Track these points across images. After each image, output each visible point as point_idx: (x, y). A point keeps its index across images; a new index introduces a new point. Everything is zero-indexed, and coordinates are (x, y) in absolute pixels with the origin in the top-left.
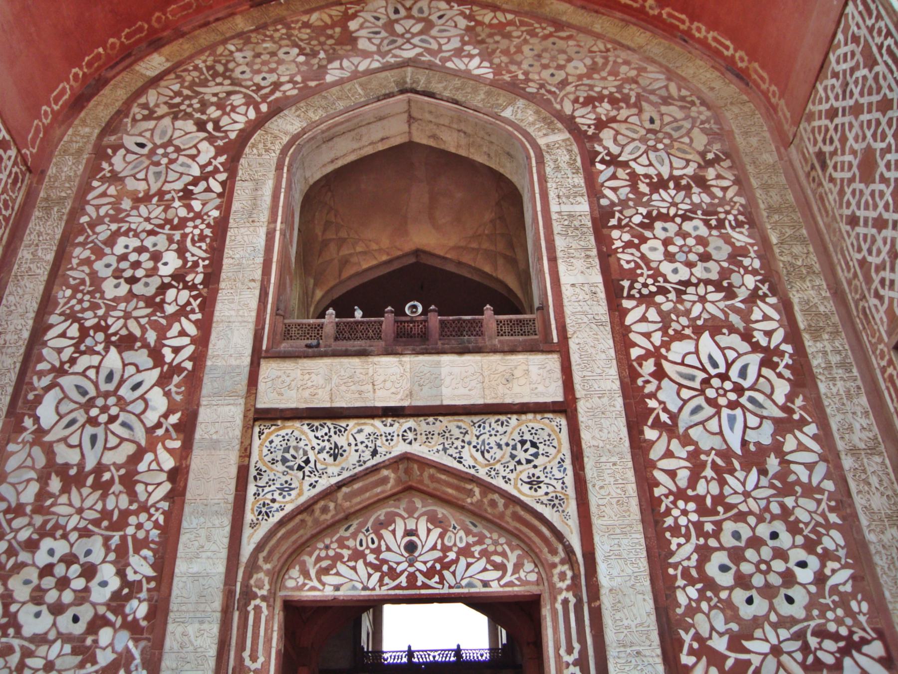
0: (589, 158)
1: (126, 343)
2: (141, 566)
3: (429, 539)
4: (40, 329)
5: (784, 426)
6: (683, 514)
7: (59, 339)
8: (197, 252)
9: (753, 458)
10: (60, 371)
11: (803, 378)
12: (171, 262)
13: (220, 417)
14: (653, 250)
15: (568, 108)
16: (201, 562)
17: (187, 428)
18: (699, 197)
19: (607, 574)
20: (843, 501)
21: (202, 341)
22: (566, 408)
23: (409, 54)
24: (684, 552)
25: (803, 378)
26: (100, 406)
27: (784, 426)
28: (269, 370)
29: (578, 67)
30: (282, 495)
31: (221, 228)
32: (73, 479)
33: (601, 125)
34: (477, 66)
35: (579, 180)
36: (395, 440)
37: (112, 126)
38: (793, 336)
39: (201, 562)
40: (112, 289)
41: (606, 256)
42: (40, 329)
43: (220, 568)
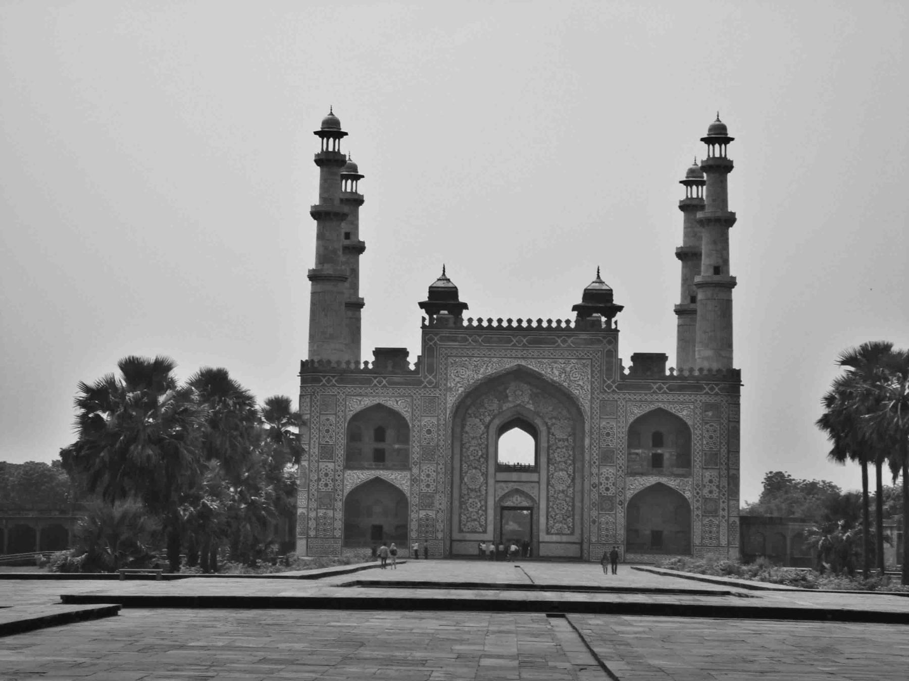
0: (549, 433)
1: (476, 468)
2: (483, 503)
3: (519, 499)
4: (461, 465)
5: (569, 487)
6: (552, 499)
7: (465, 466)
8: (484, 451)
9: (563, 492)
10: (466, 473)
11: (573, 480)
12: (480, 453)
13: (491, 481)
14: (556, 455)
15: (547, 420)
16: (491, 503)
17: (487, 483)
18: (566, 443)
19: (541, 506)
20: (573, 499)
21: (487, 468)
22: (538, 482)
23: (518, 402)
24: (551, 504)
25: (573, 480)
26: (473, 478)
27: (569, 487)
28: (498, 474)
29: (550, 408)
30: (501, 493)
31: (487, 446)
32: (472, 490)
33: (553, 424)
34: (531, 407)
35: (546, 439)
36: (516, 486)
37: (464, 419)
38: (574, 473)
39: (491, 503)
40: (472, 458)
41: (548, 455)
42: (461, 465)
43: (493, 503)
